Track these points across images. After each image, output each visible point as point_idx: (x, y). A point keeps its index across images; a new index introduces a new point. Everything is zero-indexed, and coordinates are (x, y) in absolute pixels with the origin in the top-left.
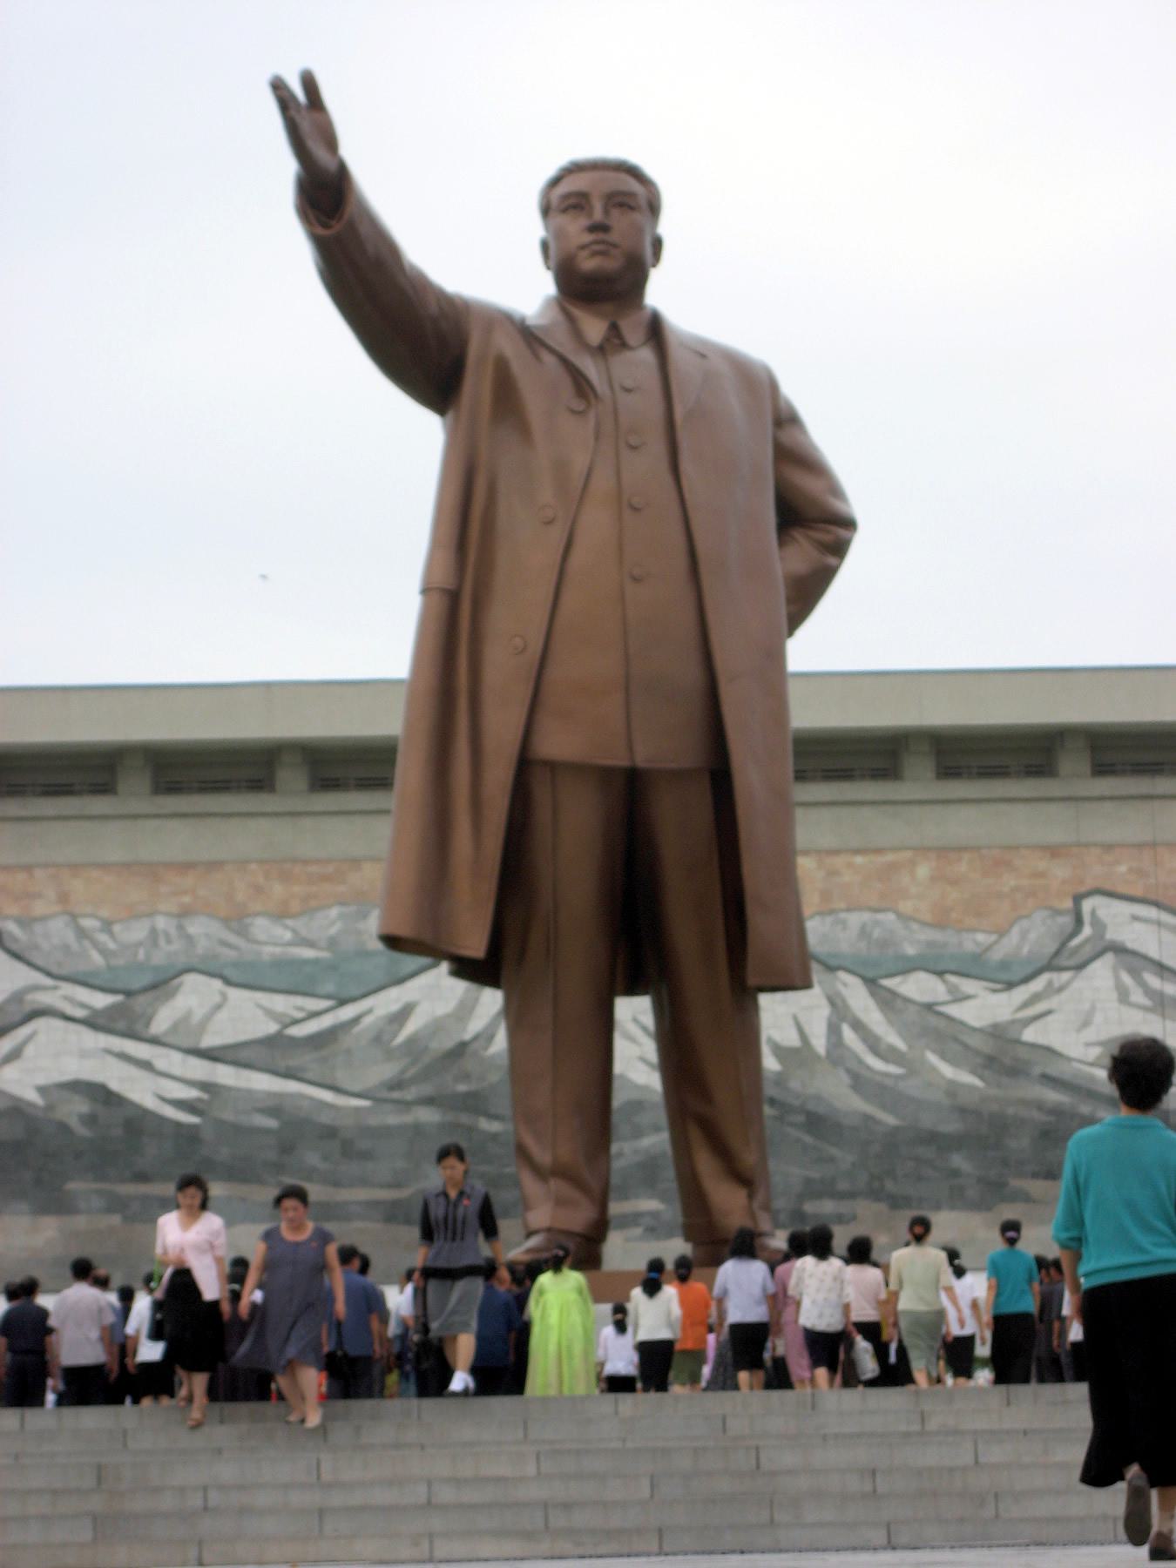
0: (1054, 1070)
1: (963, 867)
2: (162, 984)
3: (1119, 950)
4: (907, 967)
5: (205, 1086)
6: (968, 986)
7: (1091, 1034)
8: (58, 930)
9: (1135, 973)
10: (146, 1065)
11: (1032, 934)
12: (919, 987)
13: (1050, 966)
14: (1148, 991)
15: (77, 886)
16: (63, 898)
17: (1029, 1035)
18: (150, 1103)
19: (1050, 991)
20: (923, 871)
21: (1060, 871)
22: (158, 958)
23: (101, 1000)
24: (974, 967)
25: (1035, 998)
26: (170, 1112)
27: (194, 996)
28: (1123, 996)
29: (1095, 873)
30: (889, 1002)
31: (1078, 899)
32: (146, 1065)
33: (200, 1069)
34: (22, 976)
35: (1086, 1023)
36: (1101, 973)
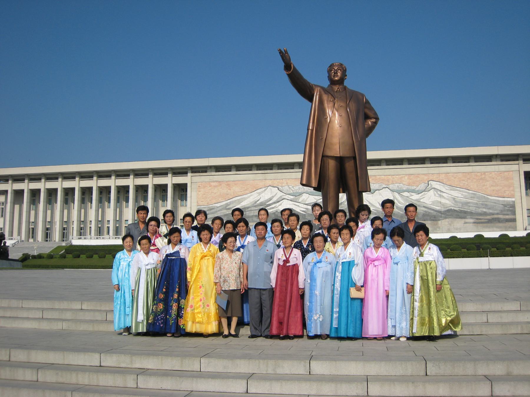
0: (425, 205)
1: (412, 177)
2: (301, 194)
3: (434, 188)
4: (404, 191)
5: (306, 209)
6: (413, 194)
7: (430, 200)
8: (286, 187)
9: (437, 192)
10: (299, 206)
11: (422, 186)
12: (406, 194)
13: (424, 191)
14: (438, 194)
15: (289, 181)
16: (287, 183)
17: (421, 201)
18: (299, 211)
19: (424, 194)
20: (406, 178)
21: (426, 178)
22: (300, 191)
23: (292, 197)
24: (413, 191)
25: (422, 195)
26: (302, 212)
27: (305, 196)
28: (435, 195)
29: (431, 178)
30: (402, 196)
31: (428, 181)
32: (299, 206)
33: (306, 206)
34: (282, 194)
35: (430, 199)
36: (432, 191)
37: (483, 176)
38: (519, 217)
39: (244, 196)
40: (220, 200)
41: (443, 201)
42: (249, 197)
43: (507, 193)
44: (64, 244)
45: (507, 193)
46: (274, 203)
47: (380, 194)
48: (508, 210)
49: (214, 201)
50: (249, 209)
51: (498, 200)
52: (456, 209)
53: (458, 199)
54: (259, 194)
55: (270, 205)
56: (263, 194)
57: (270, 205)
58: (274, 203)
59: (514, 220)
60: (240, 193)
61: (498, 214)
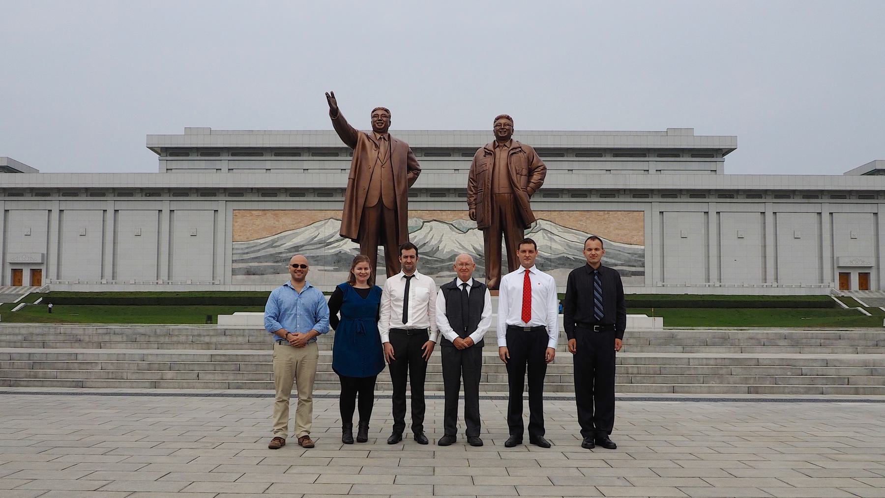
28: (544, 238)
37: (607, 216)
38: (647, 270)
39: (298, 231)
40: (264, 234)
41: (554, 246)
42: (303, 232)
43: (635, 238)
44: (36, 290)
45: (635, 238)
46: (337, 241)
47: (475, 234)
48: (636, 261)
49: (257, 236)
50: (304, 248)
51: (624, 248)
52: (571, 257)
53: (572, 244)
54: (318, 228)
55: (331, 243)
56: (322, 229)
57: (331, 243)
58: (337, 241)
59: (642, 274)
60: (291, 227)
61: (622, 265)
